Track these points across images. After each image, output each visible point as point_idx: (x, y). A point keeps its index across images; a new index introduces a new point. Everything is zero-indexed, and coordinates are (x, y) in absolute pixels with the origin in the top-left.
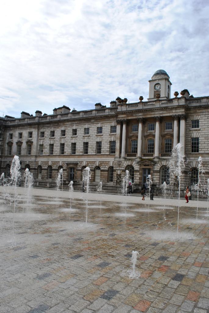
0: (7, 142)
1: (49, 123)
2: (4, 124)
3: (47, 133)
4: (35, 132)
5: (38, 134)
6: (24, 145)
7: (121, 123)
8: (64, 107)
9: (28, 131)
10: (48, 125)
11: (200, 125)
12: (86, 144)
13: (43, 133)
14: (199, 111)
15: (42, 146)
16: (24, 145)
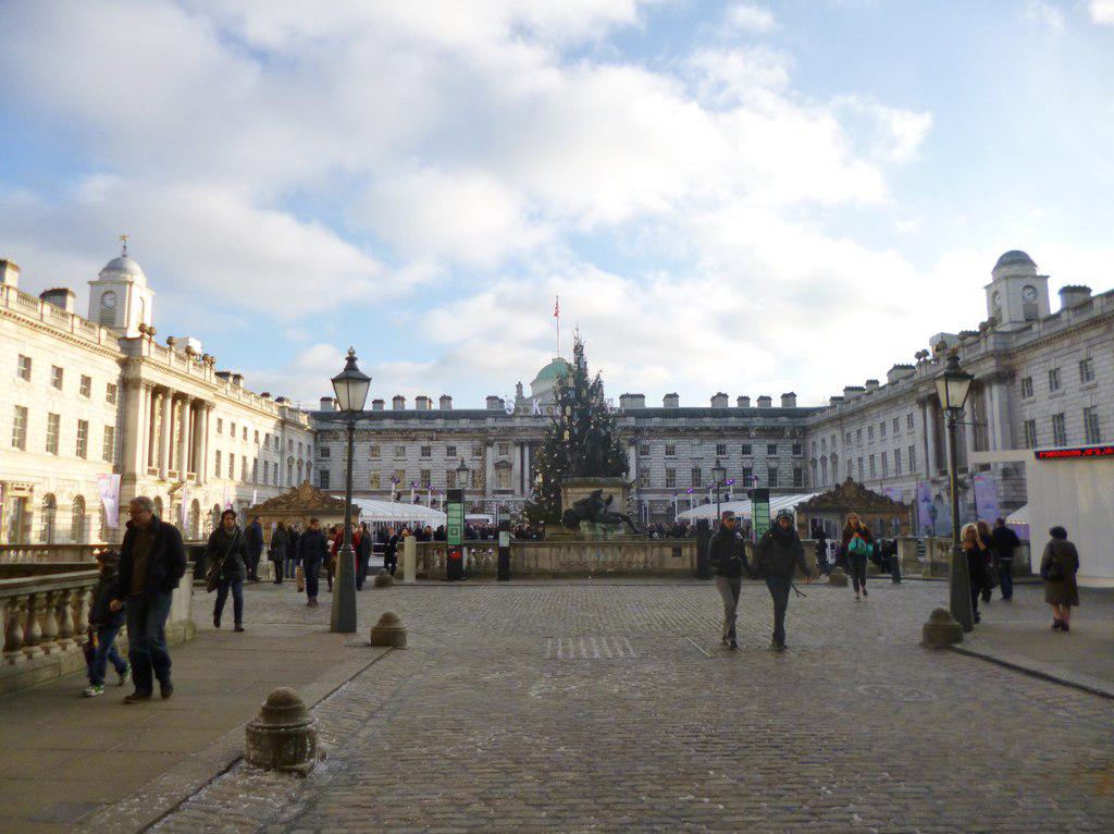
0: (810, 459)
1: (852, 414)
2: (801, 424)
3: (854, 436)
4: (837, 432)
5: (843, 440)
6: (829, 463)
7: (922, 403)
8: (897, 367)
9: (830, 434)
10: (851, 419)
11: (1035, 389)
12: (897, 452)
13: (848, 435)
14: (1029, 356)
15: (850, 462)
16: (829, 463)
